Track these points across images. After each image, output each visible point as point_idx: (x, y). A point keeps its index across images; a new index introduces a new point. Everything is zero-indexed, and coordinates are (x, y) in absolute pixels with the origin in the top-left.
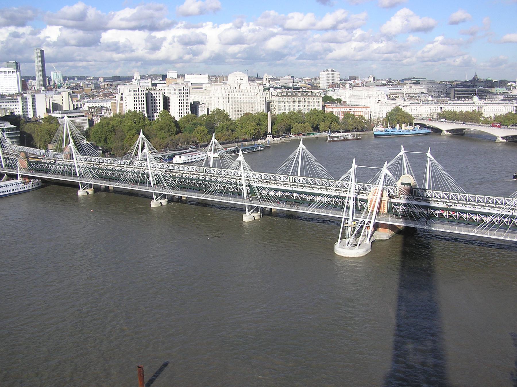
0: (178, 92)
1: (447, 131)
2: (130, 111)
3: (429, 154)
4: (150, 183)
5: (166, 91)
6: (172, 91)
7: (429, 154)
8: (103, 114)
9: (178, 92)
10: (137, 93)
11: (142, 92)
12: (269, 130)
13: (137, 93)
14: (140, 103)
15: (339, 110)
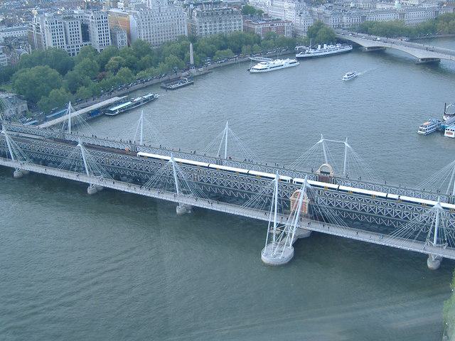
0: (97, 21)
1: (369, 48)
2: (49, 47)
3: (347, 145)
4: (85, 169)
5: (84, 18)
6: (91, 20)
7: (347, 145)
8: (21, 50)
9: (97, 21)
10: (55, 25)
11: (60, 25)
12: (192, 62)
13: (55, 25)
14: (59, 35)
15: (261, 27)
